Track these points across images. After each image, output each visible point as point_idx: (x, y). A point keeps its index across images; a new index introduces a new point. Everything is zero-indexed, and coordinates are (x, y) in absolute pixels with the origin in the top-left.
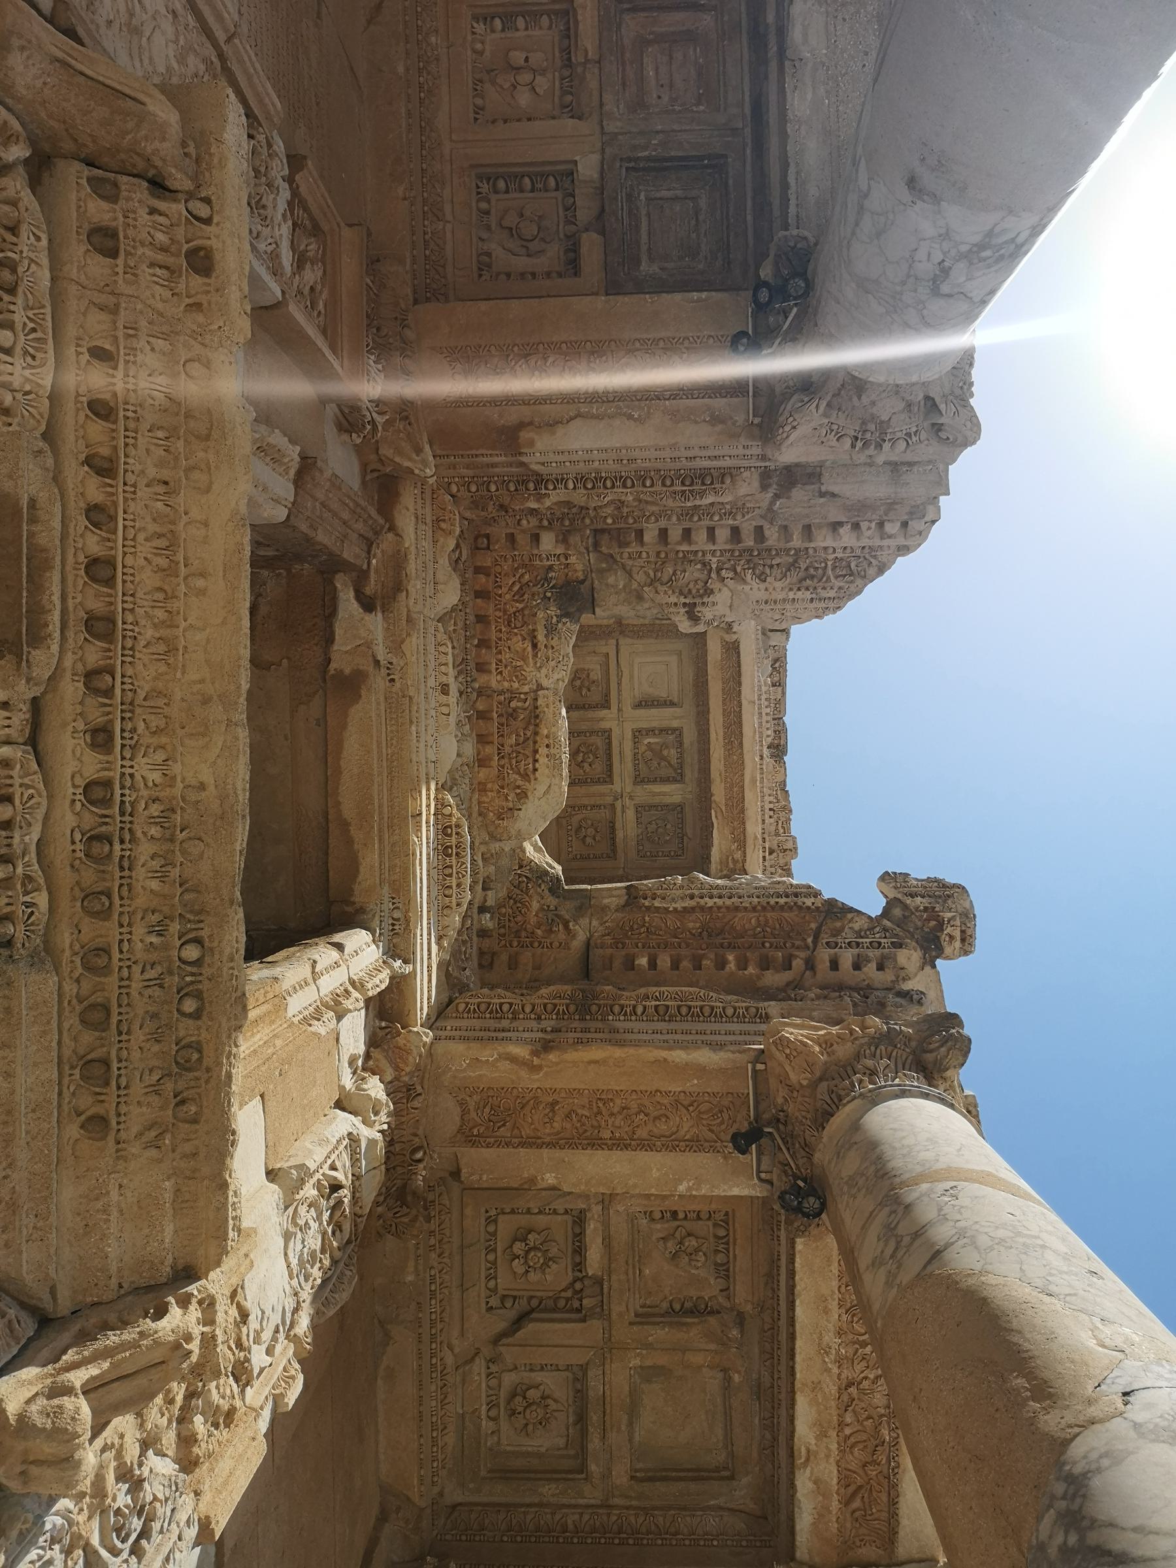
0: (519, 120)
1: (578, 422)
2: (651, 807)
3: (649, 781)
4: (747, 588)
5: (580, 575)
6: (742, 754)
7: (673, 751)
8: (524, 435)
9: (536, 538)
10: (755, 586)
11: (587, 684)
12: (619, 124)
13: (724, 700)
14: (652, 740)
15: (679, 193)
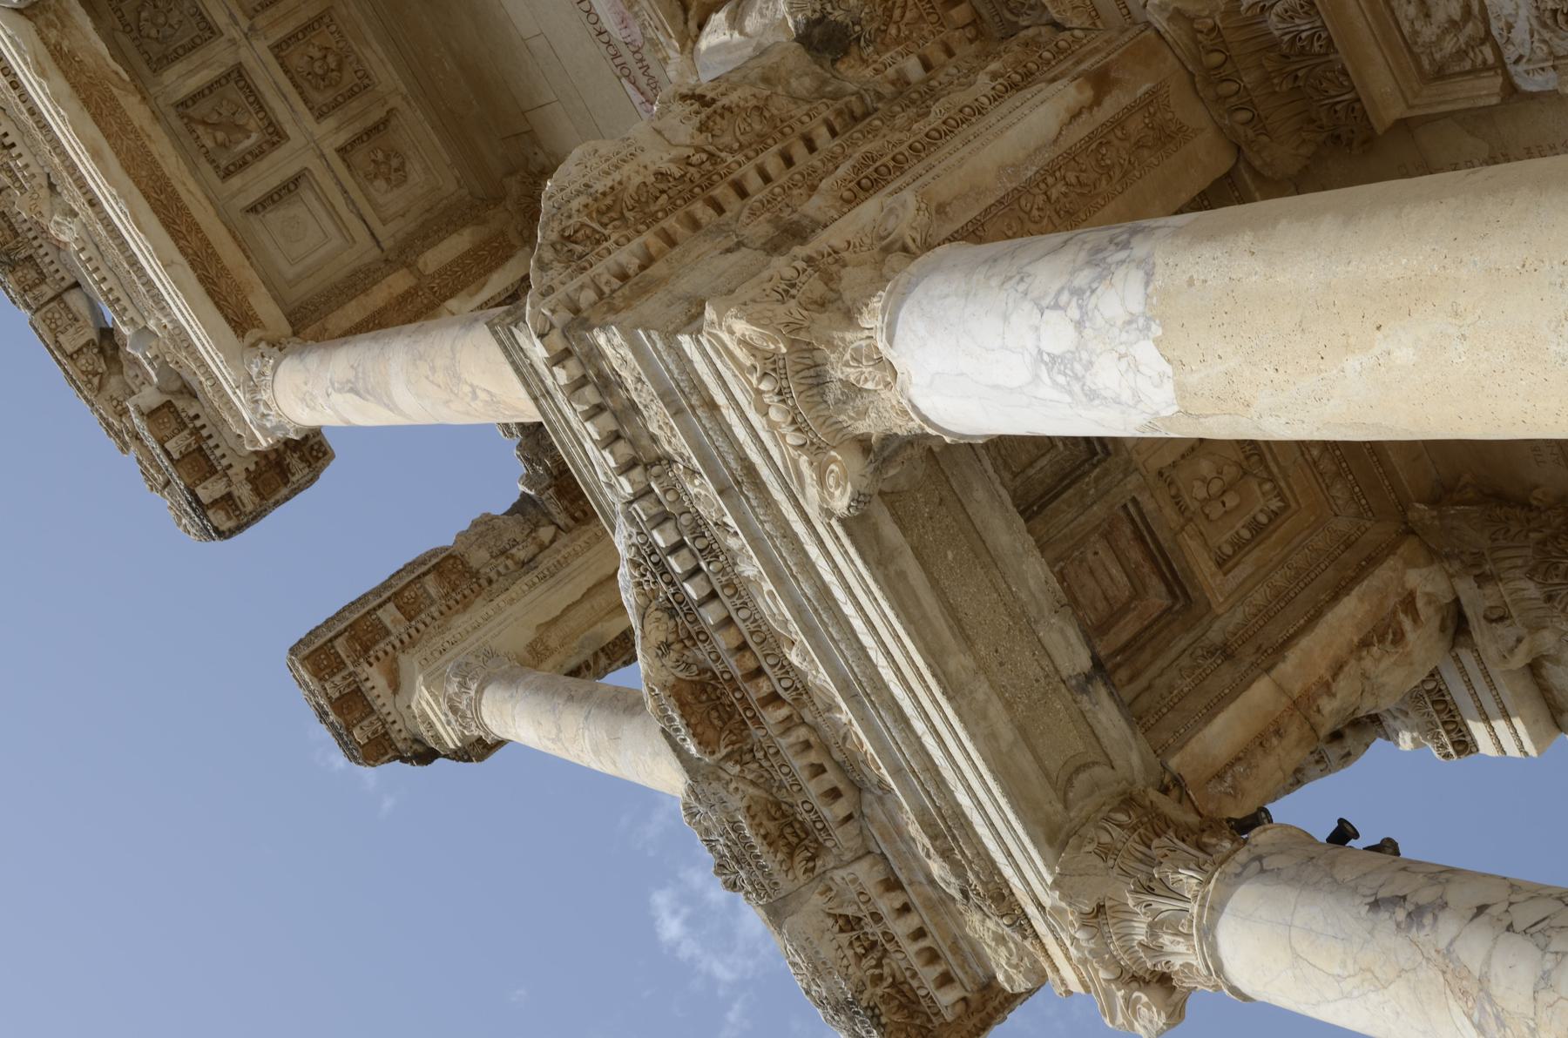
0: (1183, 457)
1: (1053, 135)
2: (193, 47)
3: (218, 82)
4: (666, 157)
5: (841, 67)
6: (138, 184)
7: (209, 144)
8: (1088, 94)
9: (927, 65)
10: (659, 164)
11: (383, 168)
12: (1129, 487)
13: (209, 244)
14: (247, 143)
15: (1031, 472)
